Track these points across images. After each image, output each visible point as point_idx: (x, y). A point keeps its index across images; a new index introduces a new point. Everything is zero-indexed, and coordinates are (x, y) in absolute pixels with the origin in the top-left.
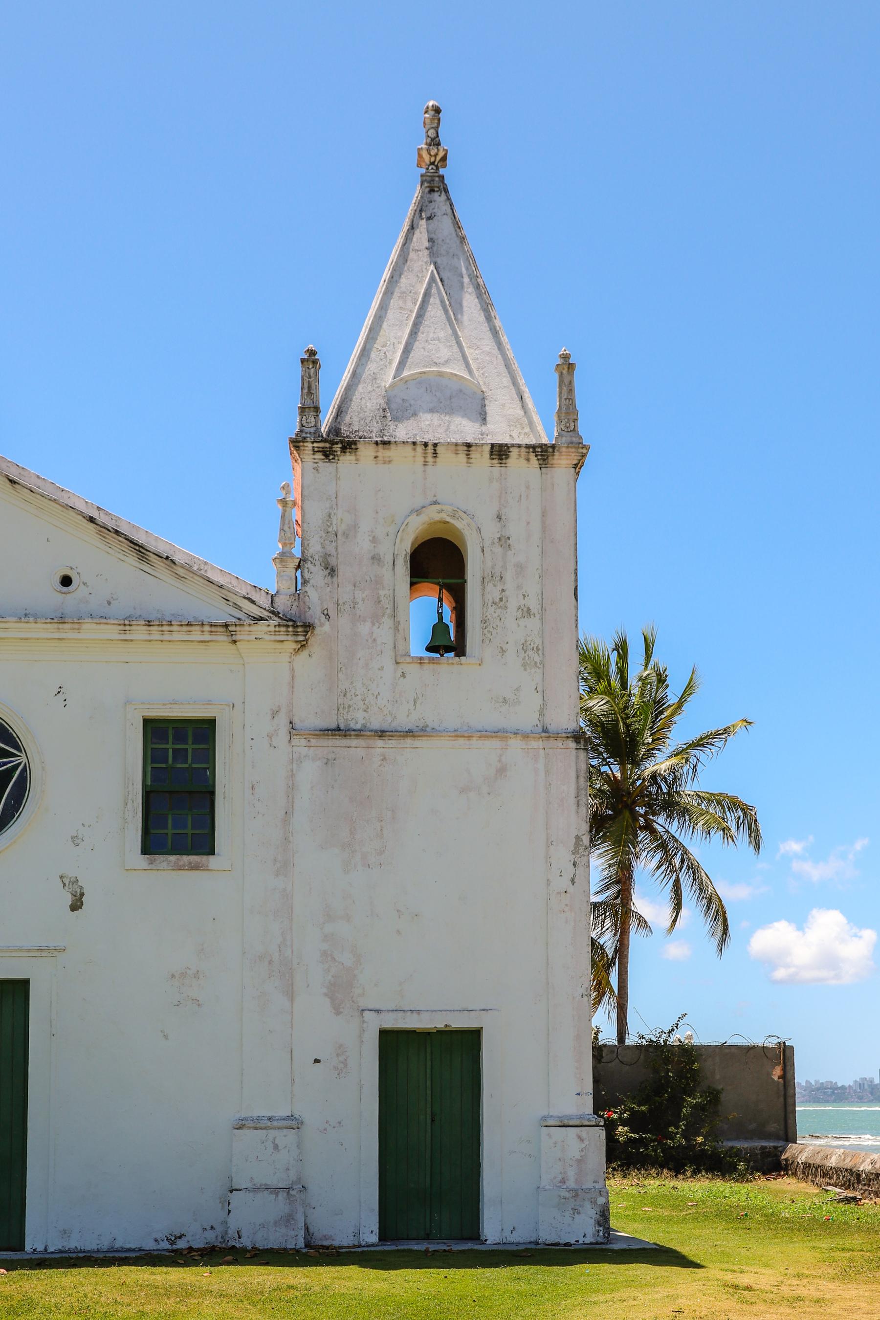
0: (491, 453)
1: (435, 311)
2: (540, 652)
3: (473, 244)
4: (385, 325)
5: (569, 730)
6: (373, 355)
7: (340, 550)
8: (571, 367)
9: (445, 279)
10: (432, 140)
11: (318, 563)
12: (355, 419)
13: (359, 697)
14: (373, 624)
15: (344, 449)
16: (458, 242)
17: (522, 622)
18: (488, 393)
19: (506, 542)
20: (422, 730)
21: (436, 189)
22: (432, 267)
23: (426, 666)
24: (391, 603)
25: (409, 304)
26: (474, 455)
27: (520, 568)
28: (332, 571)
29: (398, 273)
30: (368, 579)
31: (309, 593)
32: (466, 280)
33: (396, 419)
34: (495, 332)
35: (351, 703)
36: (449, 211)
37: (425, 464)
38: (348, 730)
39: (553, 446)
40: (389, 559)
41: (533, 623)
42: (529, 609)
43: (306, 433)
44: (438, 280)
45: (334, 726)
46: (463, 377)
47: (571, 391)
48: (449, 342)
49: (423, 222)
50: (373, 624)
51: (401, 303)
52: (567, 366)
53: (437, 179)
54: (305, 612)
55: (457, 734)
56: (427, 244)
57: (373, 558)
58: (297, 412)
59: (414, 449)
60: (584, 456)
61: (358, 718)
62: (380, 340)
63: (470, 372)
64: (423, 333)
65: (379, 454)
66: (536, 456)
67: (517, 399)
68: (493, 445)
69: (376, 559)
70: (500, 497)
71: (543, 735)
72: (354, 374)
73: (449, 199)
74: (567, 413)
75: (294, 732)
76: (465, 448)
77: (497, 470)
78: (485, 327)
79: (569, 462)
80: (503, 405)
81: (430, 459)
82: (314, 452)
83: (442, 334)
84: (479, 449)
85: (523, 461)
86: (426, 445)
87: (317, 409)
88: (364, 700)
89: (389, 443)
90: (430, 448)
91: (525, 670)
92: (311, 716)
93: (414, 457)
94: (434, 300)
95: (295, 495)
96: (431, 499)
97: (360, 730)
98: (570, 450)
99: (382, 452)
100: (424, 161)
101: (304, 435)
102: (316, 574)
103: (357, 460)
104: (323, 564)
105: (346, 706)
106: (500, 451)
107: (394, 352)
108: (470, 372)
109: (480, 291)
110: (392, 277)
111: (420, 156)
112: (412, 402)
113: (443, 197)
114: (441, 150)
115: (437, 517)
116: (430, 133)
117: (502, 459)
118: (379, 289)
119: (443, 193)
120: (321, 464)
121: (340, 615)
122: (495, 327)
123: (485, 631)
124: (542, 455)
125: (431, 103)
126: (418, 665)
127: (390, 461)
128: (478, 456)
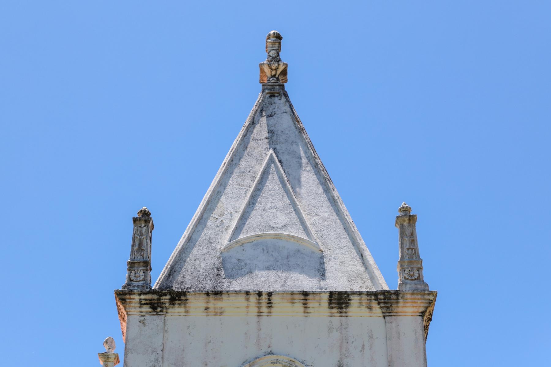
0: (330, 302)
1: (273, 185)
3: (311, 133)
4: (223, 199)
6: (210, 223)
8: (412, 219)
9: (283, 160)
10: (273, 58)
12: (188, 278)
15: (172, 301)
16: (297, 133)
18: (327, 252)
21: (276, 95)
22: (271, 151)
25: (248, 181)
26: (312, 304)
29: (238, 157)
32: (305, 161)
33: (230, 276)
34: (333, 202)
36: (288, 109)
37: (260, 314)
39: (397, 293)
43: (134, 286)
46: (300, 239)
47: (413, 241)
48: (287, 209)
49: (264, 120)
51: (239, 180)
52: (407, 219)
53: (277, 87)
56: (266, 135)
58: (126, 266)
59: (248, 299)
60: (431, 303)
63: (308, 233)
64: (261, 203)
65: (210, 305)
66: (379, 304)
67: (357, 257)
68: (331, 293)
70: (341, 347)
72: (190, 239)
73: (288, 101)
74: (411, 262)
76: (302, 297)
77: (337, 320)
78: (324, 198)
79: (415, 309)
80: (343, 263)
81: (264, 309)
82: (141, 305)
83: (280, 204)
84: (317, 298)
85: (364, 310)
86: (260, 294)
87: (147, 264)
89: (221, 293)
90: (264, 297)
93: (247, 307)
94: (273, 177)
95: (119, 349)
96: (265, 349)
98: (415, 296)
99: (214, 303)
100: (266, 76)
101: (132, 288)
103: (187, 312)
106: (339, 299)
107: (231, 220)
108: (308, 233)
109: (317, 169)
110: (232, 160)
112: (248, 262)
113: (283, 99)
114: (281, 64)
116: (271, 54)
117: (341, 308)
118: (219, 170)
119: (283, 97)
120: (148, 317)
122: (333, 197)
124: (385, 303)
125: (272, 32)
127: (221, 313)
128: (316, 305)
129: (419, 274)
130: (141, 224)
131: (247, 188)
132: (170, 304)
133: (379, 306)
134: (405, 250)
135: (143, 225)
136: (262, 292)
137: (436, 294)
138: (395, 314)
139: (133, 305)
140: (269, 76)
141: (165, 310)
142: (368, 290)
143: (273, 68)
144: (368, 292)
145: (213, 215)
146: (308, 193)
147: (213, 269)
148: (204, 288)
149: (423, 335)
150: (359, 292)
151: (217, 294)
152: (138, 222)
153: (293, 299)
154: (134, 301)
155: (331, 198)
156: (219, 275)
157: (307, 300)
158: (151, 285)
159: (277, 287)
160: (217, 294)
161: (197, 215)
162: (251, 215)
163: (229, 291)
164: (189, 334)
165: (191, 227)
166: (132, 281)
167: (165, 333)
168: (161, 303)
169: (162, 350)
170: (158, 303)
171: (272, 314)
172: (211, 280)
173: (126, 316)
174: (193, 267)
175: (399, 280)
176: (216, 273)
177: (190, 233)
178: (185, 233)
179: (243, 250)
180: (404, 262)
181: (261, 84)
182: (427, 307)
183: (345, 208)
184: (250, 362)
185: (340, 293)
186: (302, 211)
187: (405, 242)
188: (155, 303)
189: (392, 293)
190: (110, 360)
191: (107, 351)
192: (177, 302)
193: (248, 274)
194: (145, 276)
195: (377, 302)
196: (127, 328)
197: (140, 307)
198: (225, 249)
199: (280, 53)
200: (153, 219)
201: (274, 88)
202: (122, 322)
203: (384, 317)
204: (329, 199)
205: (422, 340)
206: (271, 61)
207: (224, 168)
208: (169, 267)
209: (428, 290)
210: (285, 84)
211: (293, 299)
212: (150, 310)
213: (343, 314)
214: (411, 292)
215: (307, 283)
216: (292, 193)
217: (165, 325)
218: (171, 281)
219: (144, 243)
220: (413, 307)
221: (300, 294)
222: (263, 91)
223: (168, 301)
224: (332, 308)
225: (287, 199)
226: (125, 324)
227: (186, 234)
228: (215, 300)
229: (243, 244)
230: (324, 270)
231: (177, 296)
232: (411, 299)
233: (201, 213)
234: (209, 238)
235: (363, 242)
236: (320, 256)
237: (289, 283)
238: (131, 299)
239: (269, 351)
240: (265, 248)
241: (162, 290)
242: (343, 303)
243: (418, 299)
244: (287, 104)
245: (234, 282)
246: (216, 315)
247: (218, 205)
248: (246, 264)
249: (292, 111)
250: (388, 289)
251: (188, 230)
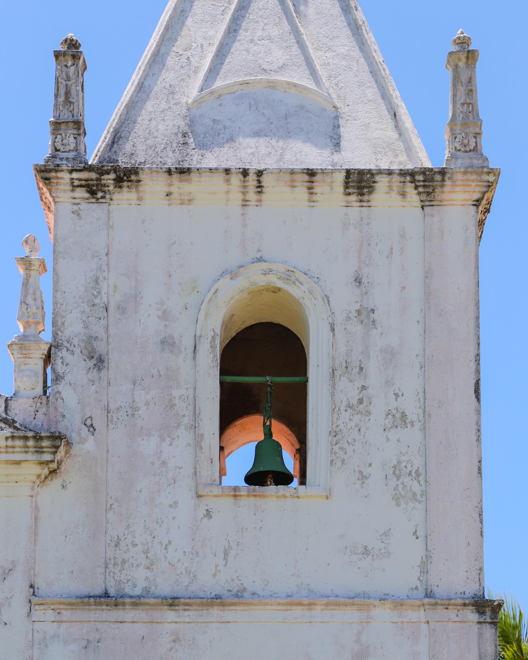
0: (347, 185)
2: (421, 478)
4: (189, 22)
5: (467, 595)
6: (170, 61)
7: (112, 331)
11: (77, 351)
12: (141, 148)
13: (140, 548)
14: (162, 439)
17: (393, 434)
18: (344, 110)
19: (368, 317)
20: (237, 596)
23: (243, 501)
24: (191, 408)
26: (320, 188)
27: (390, 355)
28: (100, 362)
30: (155, 373)
31: (64, 394)
33: (201, 146)
34: (355, 29)
35: (126, 556)
37: (245, 203)
38: (122, 597)
39: (443, 172)
40: (188, 343)
41: (411, 436)
42: (404, 415)
45: (99, 590)
46: (305, 88)
50: (162, 439)
54: (57, 422)
55: (291, 601)
57: (163, 342)
59: (228, 181)
60: (490, 186)
61: (137, 580)
62: (181, 42)
63: (317, 80)
64: (246, 31)
66: (416, 187)
67: (388, 117)
68: (348, 172)
69: (168, 343)
71: (426, 600)
72: (141, 87)
75: (34, 600)
76: (306, 178)
77: (355, 211)
78: (341, 22)
79: (467, 196)
80: (367, 126)
81: (252, 196)
83: (275, 32)
84: (328, 179)
85: (395, 196)
86: (245, 173)
88: (146, 552)
90: (252, 178)
91: (398, 505)
92: (62, 576)
93: (228, 192)
95: (44, 252)
97: (139, 597)
98: (469, 176)
99: (179, 186)
102: (73, 366)
103: (140, 199)
104: (86, 352)
105: (119, 561)
107: (202, 58)
108: (317, 80)
112: (228, 124)
115: (262, 281)
117: (362, 194)
121: (111, 426)
122: (355, 21)
123: (336, 448)
124: (424, 186)
126: (232, 499)
127: (190, 201)
128: (326, 189)
129: (476, 143)
130: (67, 61)
131: (226, 5)
132: (115, 187)
133: (416, 192)
134: (458, 105)
135: (70, 63)
136: (248, 169)
137: (499, 172)
138: (438, 203)
139: (61, 187)
141: (108, 196)
142: (402, 167)
144: (401, 170)
145: (174, 49)
146: (318, 14)
147: (176, 134)
148: (164, 164)
149: (476, 234)
150: (388, 170)
151: (184, 172)
152: (61, 58)
153: (293, 181)
154: (62, 181)
155: (352, 22)
156: (185, 144)
157: (313, 182)
158: (87, 157)
159: (269, 163)
160: (184, 172)
161: (150, 48)
162: (233, 50)
163: (201, 168)
164: (145, 231)
165: (143, 68)
166: (59, 150)
167: (110, 230)
168: (102, 185)
169: (107, 254)
170: (97, 185)
171: (263, 203)
172: (174, 151)
173: (53, 204)
174: (147, 131)
175: (447, 152)
176: (181, 140)
177: (141, 78)
178: (133, 77)
179: (221, 105)
180: (456, 125)
182: (485, 193)
183: (373, 39)
184: (231, 272)
185: (361, 173)
186: (308, 44)
187: (459, 94)
188: (93, 185)
189: (435, 172)
190: (33, 268)
191: (28, 254)
192: (125, 184)
193: (227, 142)
194: (76, 143)
195: (413, 185)
196: (55, 221)
197: (73, 191)
198: (193, 103)
200: (84, 53)
202: (47, 212)
203: (423, 207)
204: (349, 25)
205: (474, 241)
208: (112, 130)
209: (487, 167)
211: (293, 181)
212: (87, 195)
213: (365, 204)
214: (462, 170)
215: (314, 157)
216: (294, 14)
217: (109, 218)
218: (115, 152)
219: (73, 92)
220: (465, 192)
221: (303, 173)
223: (112, 182)
224: (349, 194)
225: (287, 24)
226: (51, 216)
227: (135, 78)
228: (180, 181)
229: (220, 96)
230: (339, 137)
231: (125, 175)
232: (463, 180)
233: (157, 46)
234: (170, 86)
235: (398, 93)
236: (333, 115)
237: (288, 156)
238: (57, 178)
239: (259, 257)
240: (252, 103)
241: (103, 166)
242: (364, 187)
243: (473, 181)
245: (208, 155)
246: (182, 204)
247: (183, 33)
248: (225, 127)
250: (430, 166)
251: (139, 72)
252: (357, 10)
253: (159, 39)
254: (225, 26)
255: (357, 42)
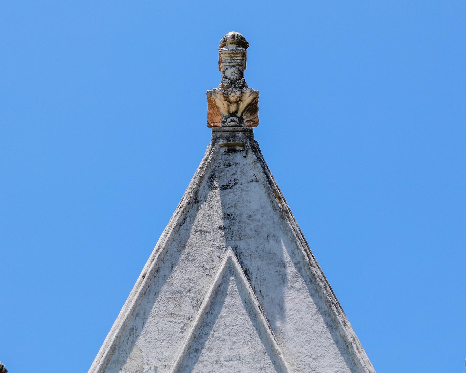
1: (233, 315)
3: (301, 219)
4: (141, 341)
16: (276, 218)
21: (238, 148)
22: (230, 253)
25: (187, 308)
29: (168, 264)
32: (291, 270)
34: (345, 347)
36: (261, 175)
44: (240, 271)
48: (259, 362)
49: (216, 194)
51: (171, 307)
53: (240, 134)
56: (221, 222)
64: (210, 350)
73: (260, 160)
78: (327, 339)
83: (245, 351)
94: (233, 304)
100: (219, 113)
109: (315, 286)
111: (212, 105)
113: (251, 157)
114: (247, 92)
116: (228, 73)
118: (134, 289)
119: (251, 152)
122: (344, 338)
125: (230, 34)
131: (185, 321)
140: (225, 114)
143: (232, 99)
155: (340, 339)
181: (211, 129)
183: (367, 359)
186: (286, 364)
199: (245, 72)
201: (234, 137)
204: (337, 342)
206: (229, 87)
207: (143, 284)
210: (254, 129)
216: (269, 331)
222: (214, 141)
225: (260, 342)
244: (259, 165)
247: (132, 354)
249: (268, 177)
252: (345, 325)
253: (104, 362)
254: (184, 346)
255: (347, 362)
